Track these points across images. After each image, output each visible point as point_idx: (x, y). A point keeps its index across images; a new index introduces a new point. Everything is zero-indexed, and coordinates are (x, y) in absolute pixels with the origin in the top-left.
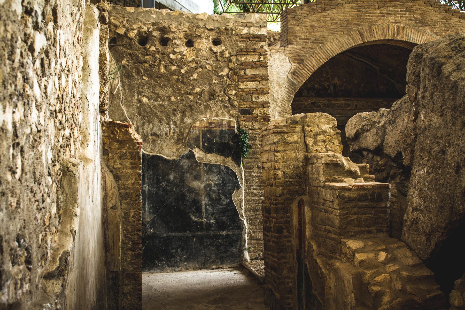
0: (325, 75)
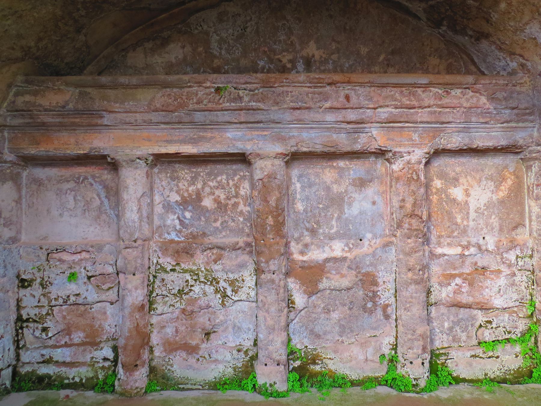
0: (282, 38)
